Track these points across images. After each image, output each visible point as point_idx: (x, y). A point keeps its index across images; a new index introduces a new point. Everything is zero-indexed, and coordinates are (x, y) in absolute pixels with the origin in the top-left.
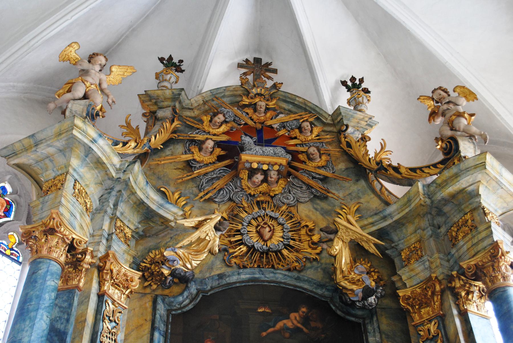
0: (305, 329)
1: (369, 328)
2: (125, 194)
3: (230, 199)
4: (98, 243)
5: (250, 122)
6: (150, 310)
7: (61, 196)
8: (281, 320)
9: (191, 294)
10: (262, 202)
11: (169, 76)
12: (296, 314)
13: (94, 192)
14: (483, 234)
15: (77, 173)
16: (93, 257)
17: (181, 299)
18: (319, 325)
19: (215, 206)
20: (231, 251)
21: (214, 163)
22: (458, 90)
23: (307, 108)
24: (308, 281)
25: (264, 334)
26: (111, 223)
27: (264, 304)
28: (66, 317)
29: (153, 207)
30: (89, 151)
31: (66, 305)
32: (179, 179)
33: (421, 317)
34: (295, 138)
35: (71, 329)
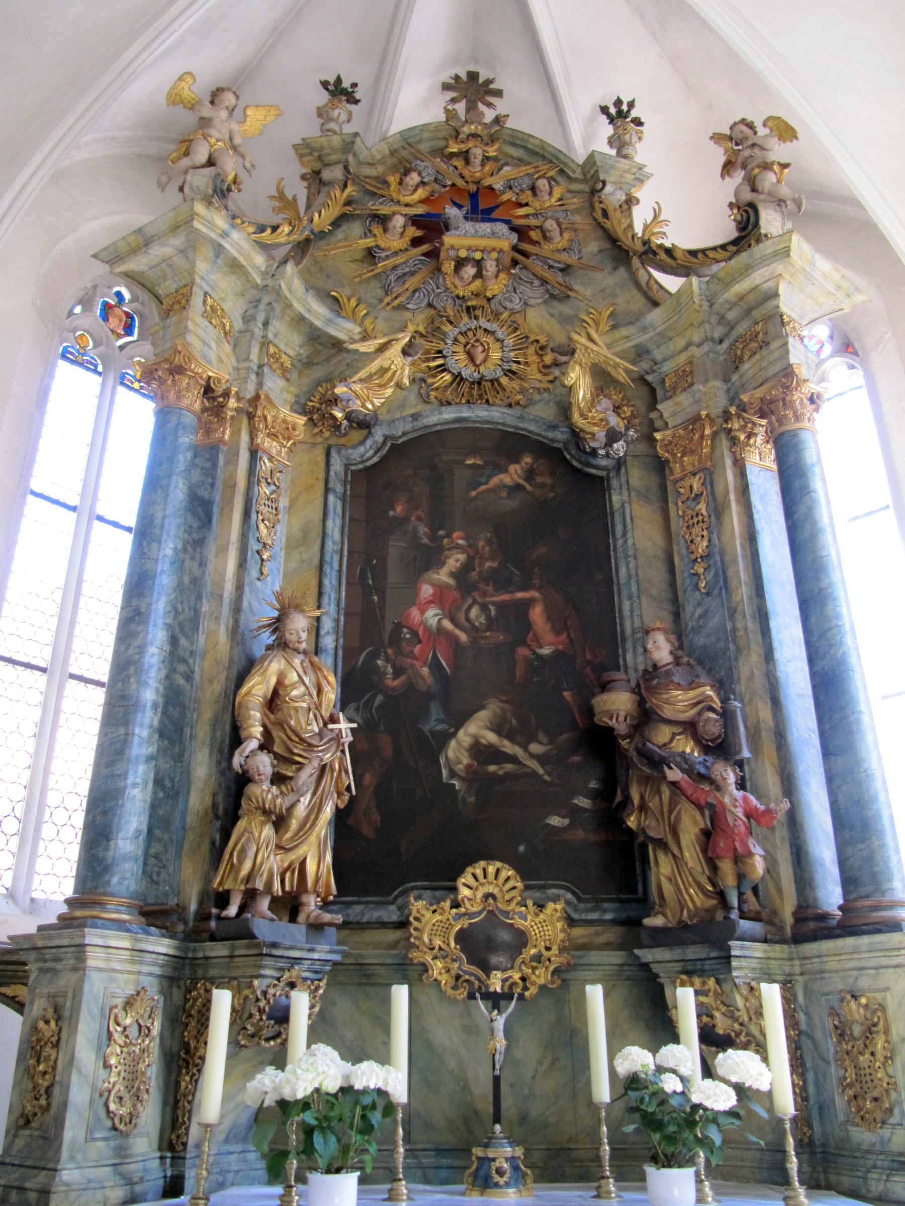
2: (278, 307)
3: (430, 305)
4: (245, 380)
5: (460, 182)
6: (322, 465)
7: (187, 319)
9: (376, 442)
10: (474, 308)
11: (336, 112)
12: (517, 467)
13: (234, 308)
14: (776, 355)
15: (207, 282)
16: (239, 399)
17: (362, 449)
18: (548, 480)
19: (409, 315)
20: (430, 381)
21: (406, 250)
22: (770, 124)
23: (546, 155)
24: (535, 421)
25: (474, 493)
26: (261, 349)
27: (474, 453)
28: (210, 481)
29: (318, 323)
30: (219, 250)
31: (208, 465)
32: (355, 277)
33: (683, 468)
34: (527, 204)
35: (218, 497)
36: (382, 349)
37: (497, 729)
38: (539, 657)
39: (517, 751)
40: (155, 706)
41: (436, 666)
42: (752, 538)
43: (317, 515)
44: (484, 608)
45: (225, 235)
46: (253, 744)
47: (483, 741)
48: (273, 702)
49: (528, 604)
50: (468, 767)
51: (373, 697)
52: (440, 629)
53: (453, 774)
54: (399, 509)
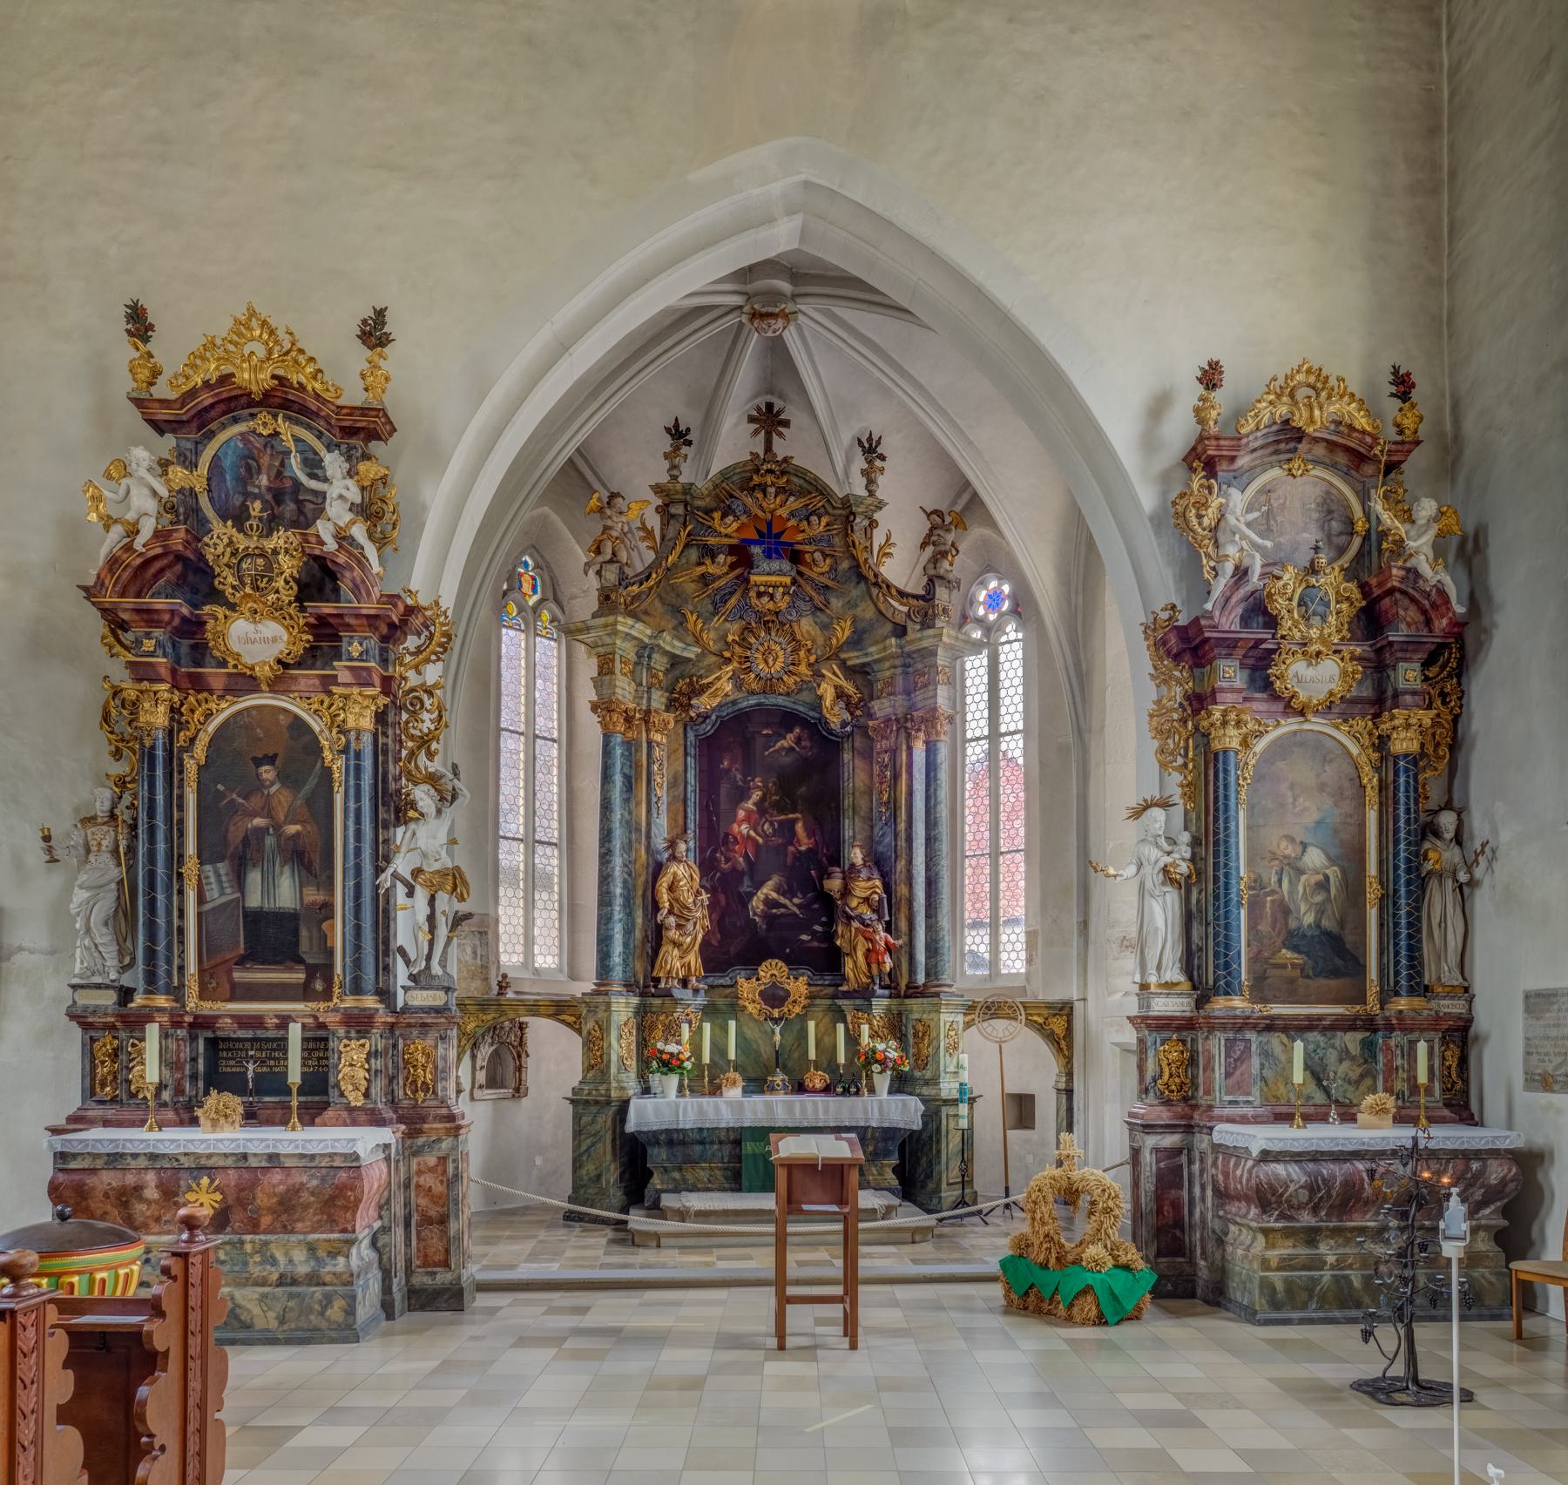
5: (760, 513)
13: (632, 656)
19: (728, 625)
27: (767, 726)
36: (718, 679)
37: (777, 891)
39: (787, 902)
41: (746, 856)
42: (910, 794)
43: (681, 768)
44: (772, 824)
49: (794, 821)
52: (749, 837)
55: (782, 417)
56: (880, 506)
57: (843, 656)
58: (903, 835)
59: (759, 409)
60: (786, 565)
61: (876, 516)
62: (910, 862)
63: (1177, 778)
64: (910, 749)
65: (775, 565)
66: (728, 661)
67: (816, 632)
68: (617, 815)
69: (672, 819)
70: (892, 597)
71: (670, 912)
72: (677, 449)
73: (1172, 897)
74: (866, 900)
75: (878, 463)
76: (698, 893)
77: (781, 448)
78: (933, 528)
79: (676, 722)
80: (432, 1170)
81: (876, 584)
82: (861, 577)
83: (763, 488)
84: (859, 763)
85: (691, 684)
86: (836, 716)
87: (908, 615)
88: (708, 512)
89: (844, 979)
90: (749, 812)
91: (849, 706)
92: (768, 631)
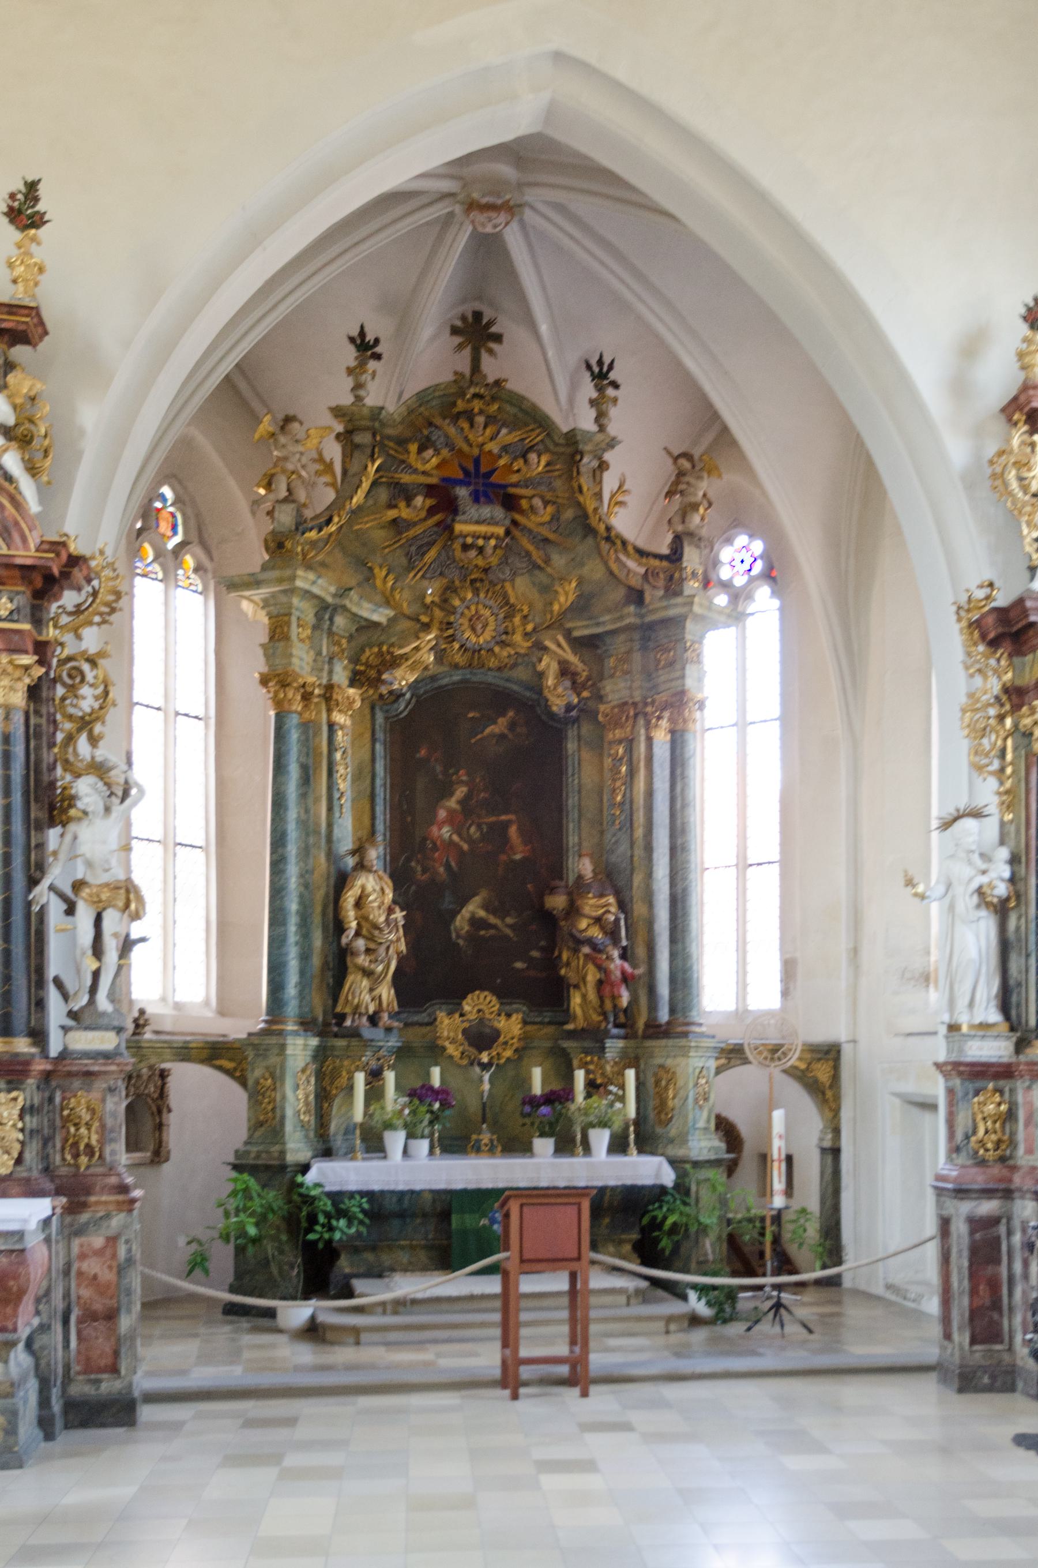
0: (510, 736)
1: (570, 733)
5: (466, 448)
6: (368, 717)
8: (488, 726)
14: (678, 674)
17: (396, 706)
19: (426, 583)
24: (519, 683)
37: (486, 907)
38: (513, 861)
40: (298, 912)
41: (448, 866)
42: (650, 794)
43: (367, 756)
44: (479, 827)
45: (314, 583)
46: (352, 933)
47: (477, 916)
48: (359, 904)
50: (467, 932)
51: (409, 887)
52: (451, 842)
53: (458, 936)
54: (423, 752)
55: (493, 329)
56: (612, 443)
57: (569, 625)
58: (640, 842)
59: (463, 318)
60: (499, 512)
61: (607, 456)
62: (649, 875)
63: (992, 783)
64: (649, 740)
65: (486, 511)
66: (426, 627)
67: (534, 595)
68: (293, 814)
69: (357, 820)
70: (628, 555)
71: (358, 934)
72: (362, 364)
73: (987, 926)
74: (598, 920)
75: (610, 392)
76: (390, 911)
77: (491, 368)
78: (681, 474)
79: (363, 700)
80: (99, 1253)
81: (608, 539)
82: (590, 531)
83: (469, 416)
84: (586, 755)
85: (380, 654)
86: (559, 697)
87: (645, 576)
88: (402, 442)
89: (567, 1015)
90: (451, 812)
91: (576, 687)
92: (476, 592)
